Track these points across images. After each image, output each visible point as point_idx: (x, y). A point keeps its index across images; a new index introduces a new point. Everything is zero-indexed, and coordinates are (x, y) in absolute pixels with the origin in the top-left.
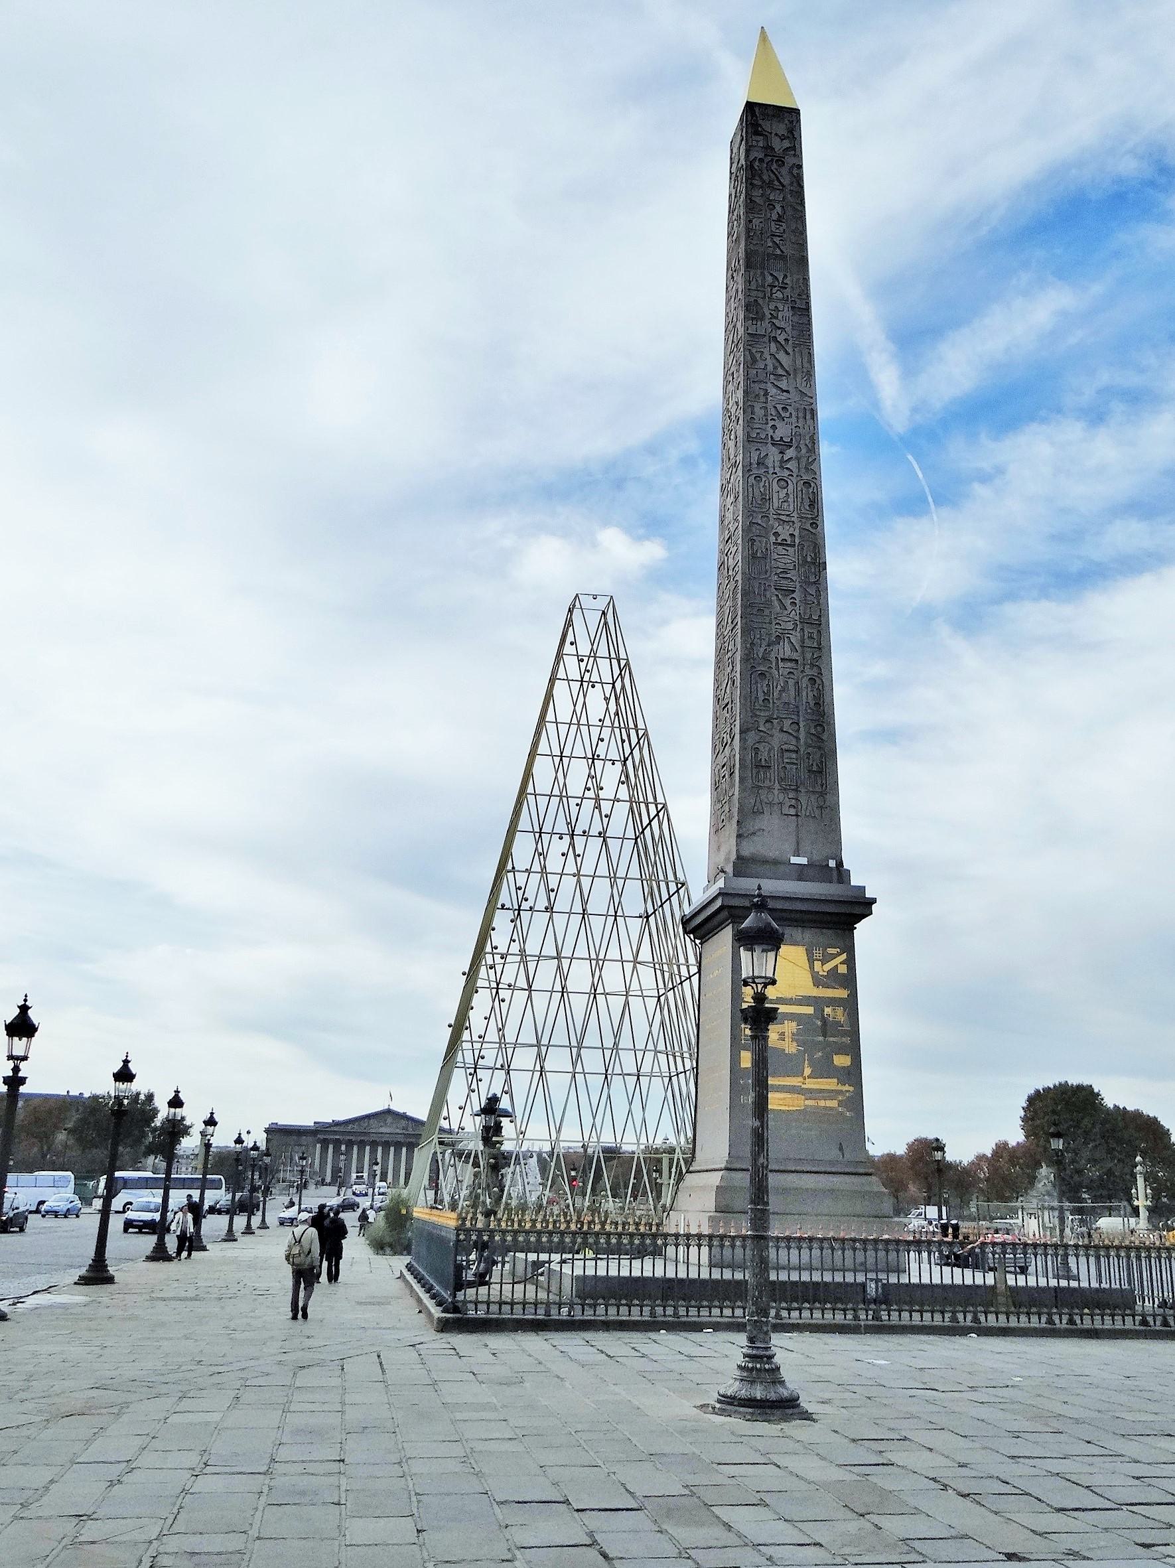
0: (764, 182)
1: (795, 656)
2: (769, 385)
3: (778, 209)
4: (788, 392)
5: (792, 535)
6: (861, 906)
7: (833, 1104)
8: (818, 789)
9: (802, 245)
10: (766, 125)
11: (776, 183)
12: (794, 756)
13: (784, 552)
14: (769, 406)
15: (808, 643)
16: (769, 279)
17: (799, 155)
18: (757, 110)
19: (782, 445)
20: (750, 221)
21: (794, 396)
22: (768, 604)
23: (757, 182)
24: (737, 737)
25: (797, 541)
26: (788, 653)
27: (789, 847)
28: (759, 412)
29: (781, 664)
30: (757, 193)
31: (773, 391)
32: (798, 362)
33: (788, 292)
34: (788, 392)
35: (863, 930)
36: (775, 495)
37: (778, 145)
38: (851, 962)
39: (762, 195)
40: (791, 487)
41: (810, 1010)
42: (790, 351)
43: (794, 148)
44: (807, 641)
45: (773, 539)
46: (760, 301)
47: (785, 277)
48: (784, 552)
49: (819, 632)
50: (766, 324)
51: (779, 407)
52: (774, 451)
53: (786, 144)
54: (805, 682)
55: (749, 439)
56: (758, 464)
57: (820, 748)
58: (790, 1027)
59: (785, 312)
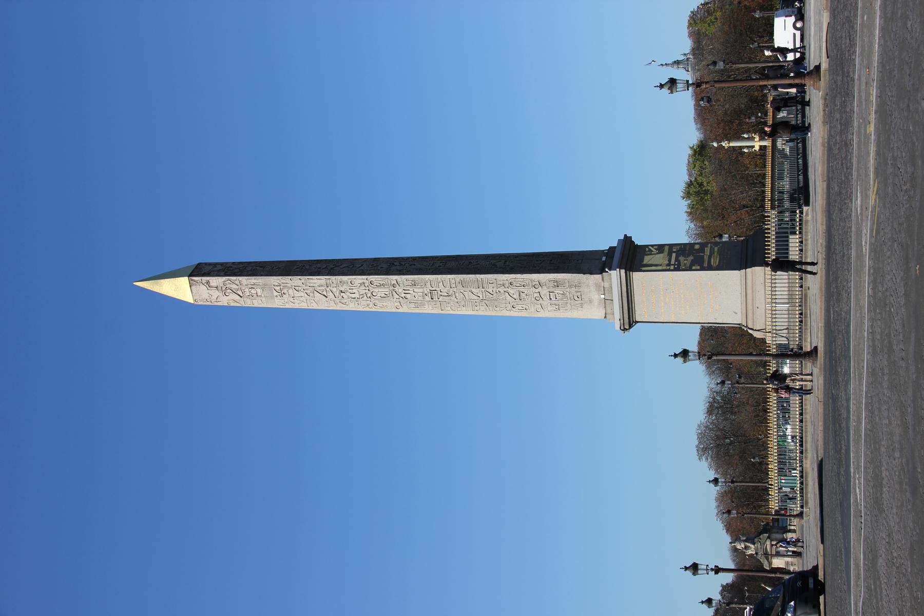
6: (627, 240)
7: (716, 249)
35: (638, 241)
37: (219, 267)
38: (652, 246)
41: (674, 255)
52: (394, 268)
58: (681, 258)
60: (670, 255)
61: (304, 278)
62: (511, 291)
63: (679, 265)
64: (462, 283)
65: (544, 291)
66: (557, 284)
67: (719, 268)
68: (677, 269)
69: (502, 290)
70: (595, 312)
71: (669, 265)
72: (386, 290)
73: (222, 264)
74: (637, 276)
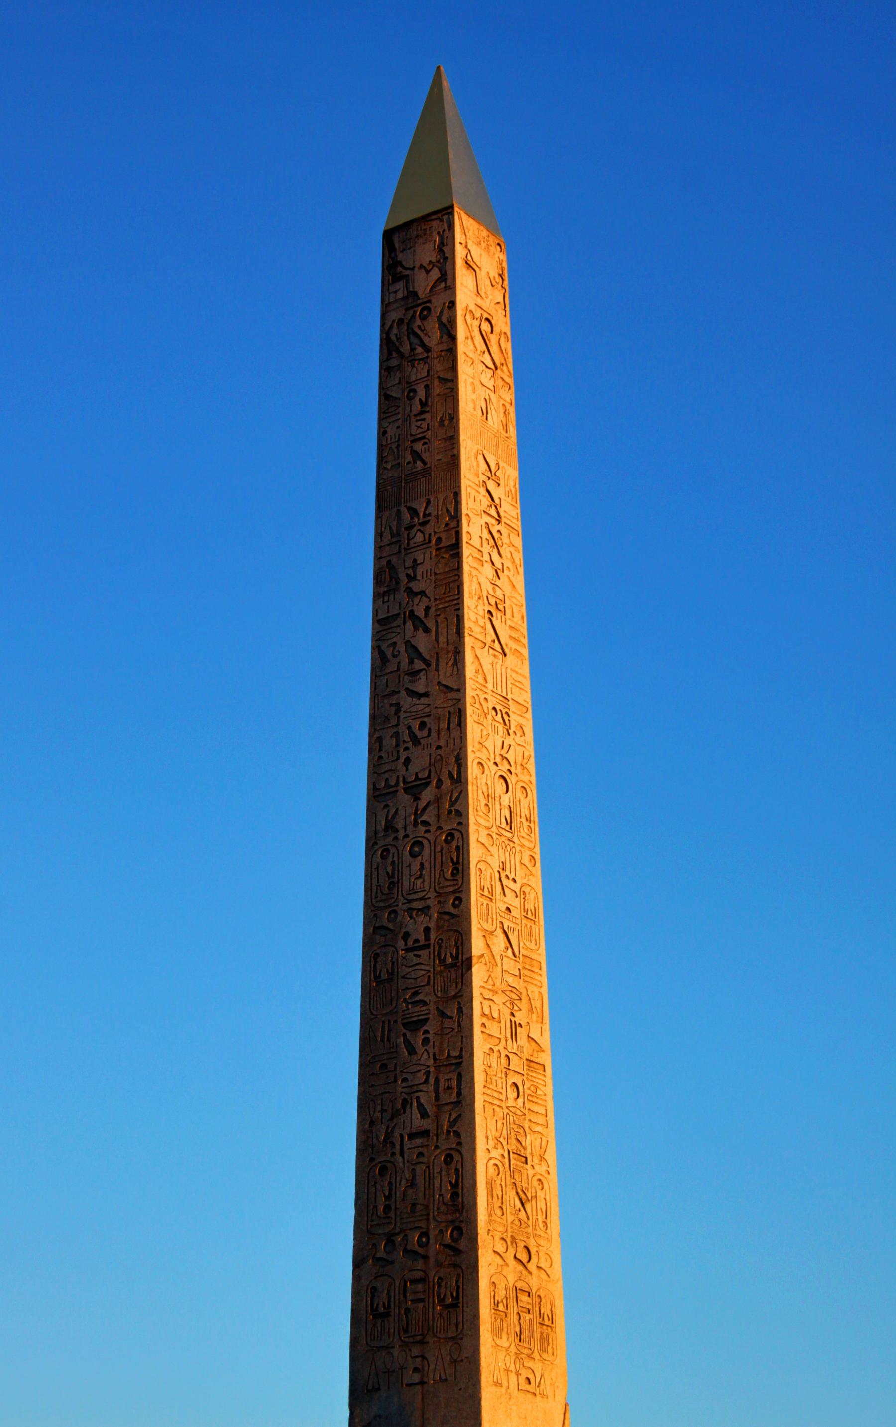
0: (401, 355)
1: (426, 1124)
2: (403, 693)
3: (421, 394)
4: (426, 695)
5: (427, 930)
8: (452, 1333)
11: (419, 349)
12: (420, 1287)
13: (415, 960)
14: (403, 730)
15: (445, 1098)
16: (406, 516)
20: (385, 433)
23: (394, 363)
25: (433, 936)
26: (418, 1123)
28: (389, 743)
29: (407, 1144)
31: (407, 702)
32: (442, 639)
33: (428, 529)
34: (426, 695)
36: (406, 871)
39: (400, 383)
40: (426, 852)
42: (431, 624)
44: (441, 1094)
45: (401, 943)
46: (394, 560)
47: (428, 502)
48: (415, 960)
49: (460, 1076)
50: (402, 596)
51: (415, 726)
56: (386, 829)
57: (455, 1265)
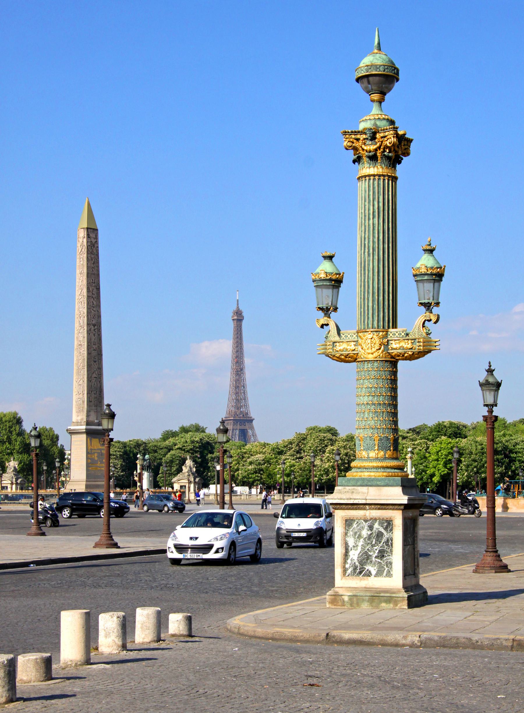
9: (98, 270)
10: (91, 235)
17: (98, 244)
18: (89, 230)
19: (94, 325)
21: (96, 312)
22: (91, 365)
24: (86, 395)
26: (96, 376)
27: (95, 418)
30: (89, 255)
31: (92, 311)
37: (94, 241)
43: (96, 242)
53: (95, 240)
54: (98, 383)
55: (88, 324)
59: (95, 290)
60: (98, 449)
61: (86, 284)
62: (81, 381)
63: (91, 454)
64: (84, 359)
65: (81, 396)
66: (83, 402)
67: (87, 470)
68: (88, 453)
69: (82, 377)
70: (75, 418)
71: (91, 449)
72: (82, 324)
73: (97, 242)
74: (84, 436)
